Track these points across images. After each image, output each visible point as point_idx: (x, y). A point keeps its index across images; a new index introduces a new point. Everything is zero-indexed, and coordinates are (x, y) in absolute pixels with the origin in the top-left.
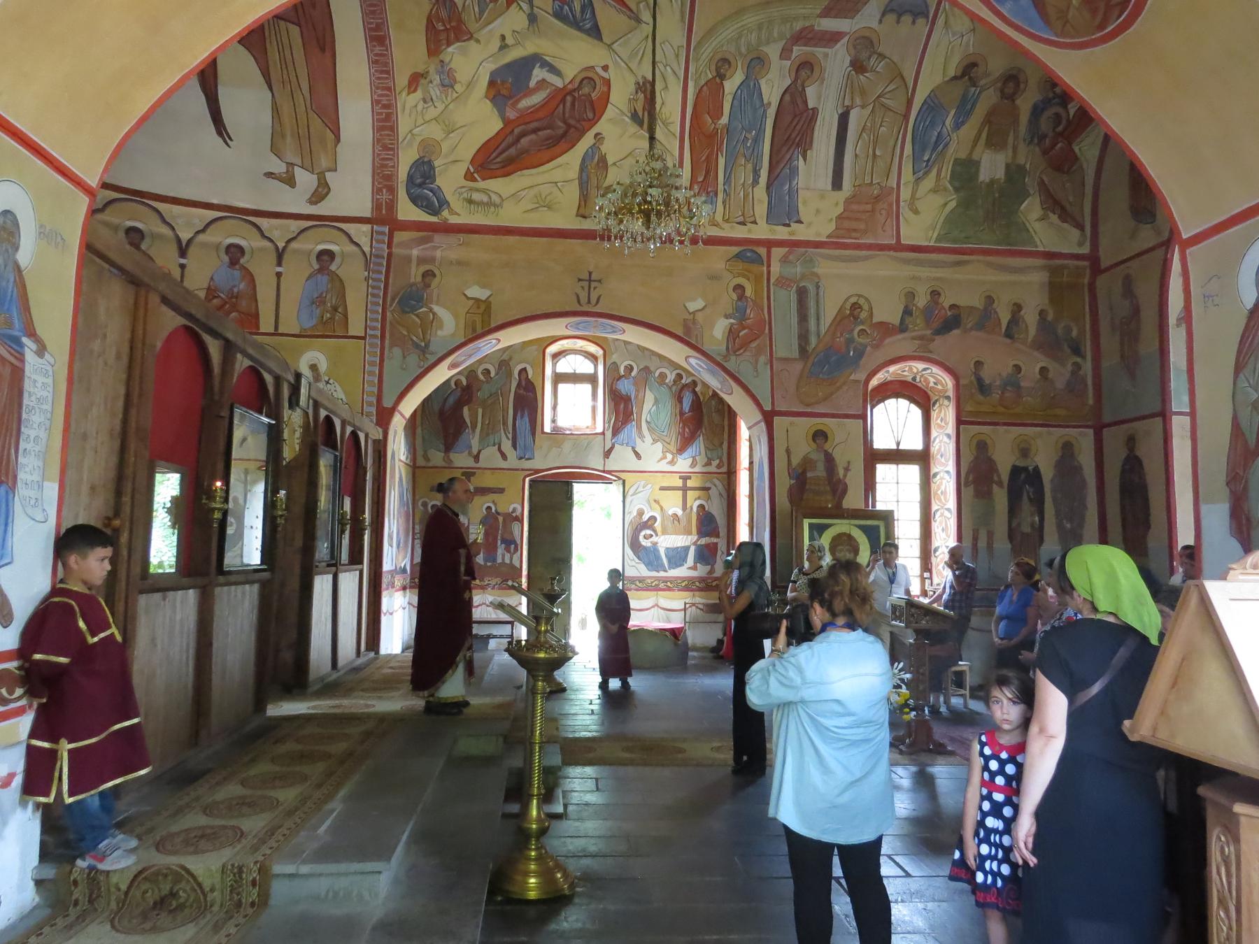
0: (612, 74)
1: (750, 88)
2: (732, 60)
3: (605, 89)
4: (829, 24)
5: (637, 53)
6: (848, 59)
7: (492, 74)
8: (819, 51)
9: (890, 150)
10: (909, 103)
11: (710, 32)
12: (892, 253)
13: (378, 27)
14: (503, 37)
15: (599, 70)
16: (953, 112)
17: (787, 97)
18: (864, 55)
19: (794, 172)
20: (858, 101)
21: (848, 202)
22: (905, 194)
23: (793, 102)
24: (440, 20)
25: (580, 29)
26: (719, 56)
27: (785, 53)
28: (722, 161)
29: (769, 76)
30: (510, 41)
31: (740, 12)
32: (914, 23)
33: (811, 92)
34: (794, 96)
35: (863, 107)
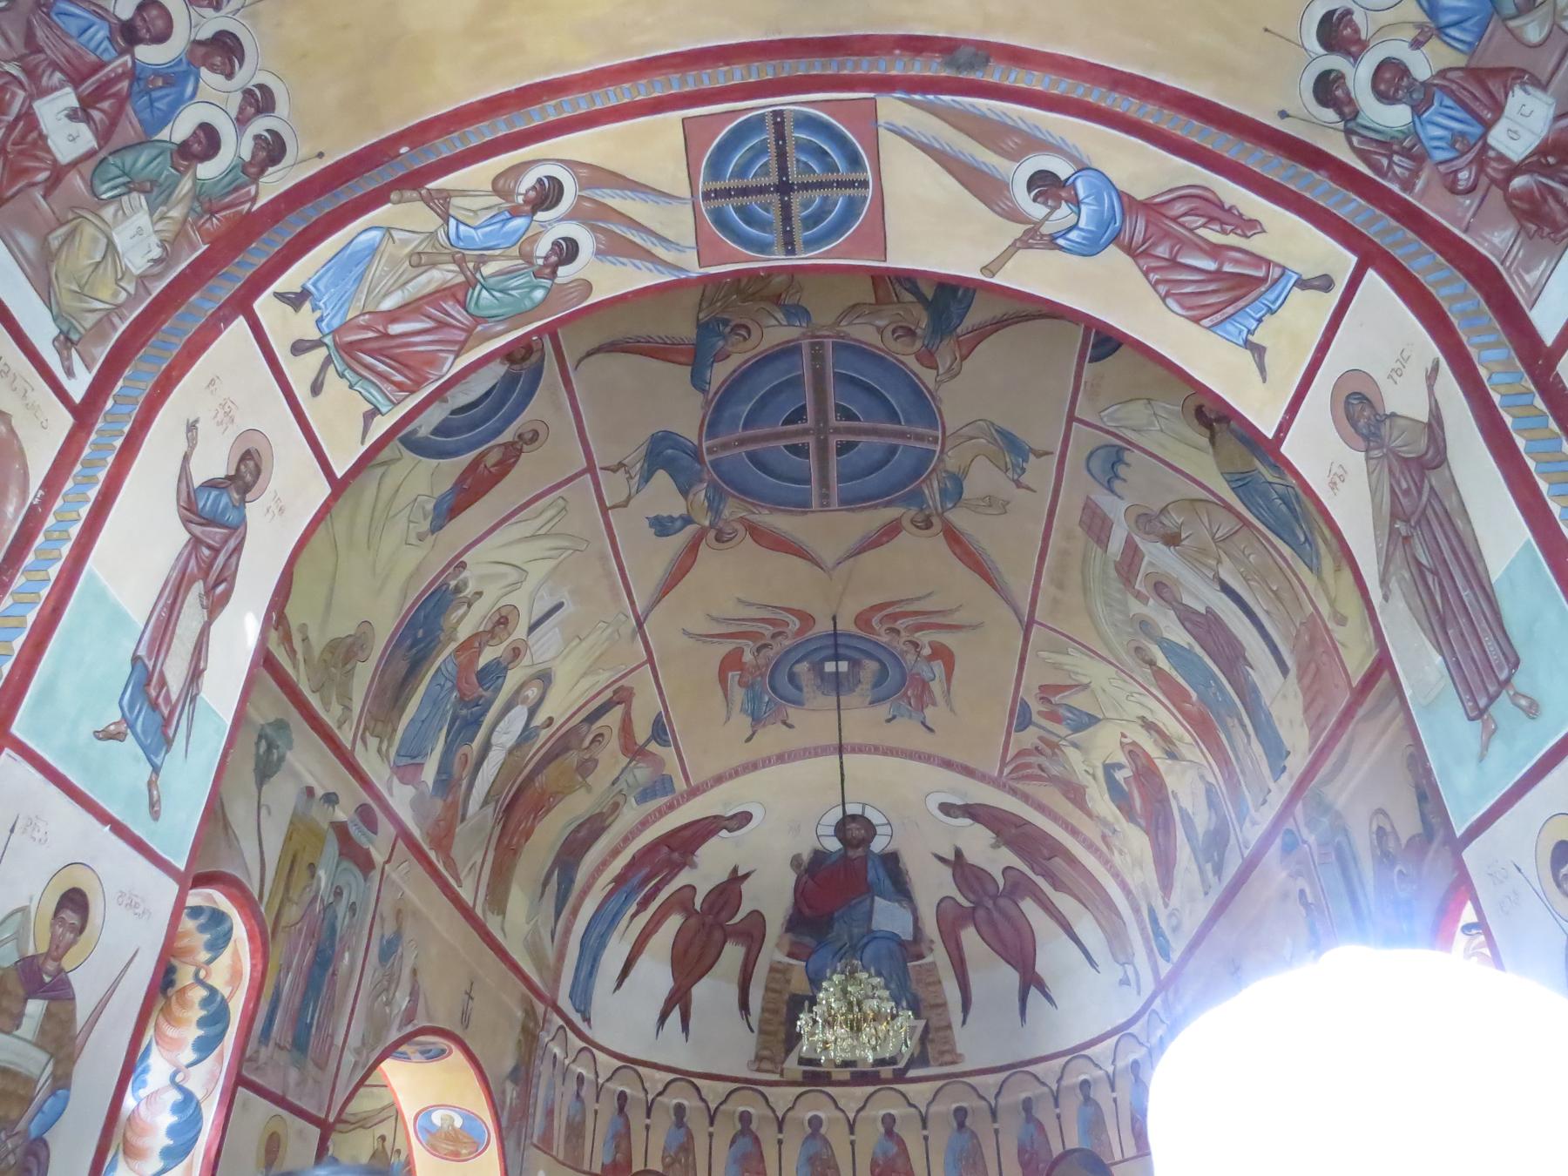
1: (1170, 649)
4: (1116, 545)
9: (1276, 570)
10: (1229, 508)
11: (1106, 644)
12: (1361, 712)
16: (1257, 463)
19: (1255, 689)
21: (1300, 679)
22: (1325, 609)
23: (1195, 624)
28: (1223, 737)
29: (1162, 626)
32: (1127, 465)
33: (1187, 600)
34: (1187, 617)
35: (1219, 562)
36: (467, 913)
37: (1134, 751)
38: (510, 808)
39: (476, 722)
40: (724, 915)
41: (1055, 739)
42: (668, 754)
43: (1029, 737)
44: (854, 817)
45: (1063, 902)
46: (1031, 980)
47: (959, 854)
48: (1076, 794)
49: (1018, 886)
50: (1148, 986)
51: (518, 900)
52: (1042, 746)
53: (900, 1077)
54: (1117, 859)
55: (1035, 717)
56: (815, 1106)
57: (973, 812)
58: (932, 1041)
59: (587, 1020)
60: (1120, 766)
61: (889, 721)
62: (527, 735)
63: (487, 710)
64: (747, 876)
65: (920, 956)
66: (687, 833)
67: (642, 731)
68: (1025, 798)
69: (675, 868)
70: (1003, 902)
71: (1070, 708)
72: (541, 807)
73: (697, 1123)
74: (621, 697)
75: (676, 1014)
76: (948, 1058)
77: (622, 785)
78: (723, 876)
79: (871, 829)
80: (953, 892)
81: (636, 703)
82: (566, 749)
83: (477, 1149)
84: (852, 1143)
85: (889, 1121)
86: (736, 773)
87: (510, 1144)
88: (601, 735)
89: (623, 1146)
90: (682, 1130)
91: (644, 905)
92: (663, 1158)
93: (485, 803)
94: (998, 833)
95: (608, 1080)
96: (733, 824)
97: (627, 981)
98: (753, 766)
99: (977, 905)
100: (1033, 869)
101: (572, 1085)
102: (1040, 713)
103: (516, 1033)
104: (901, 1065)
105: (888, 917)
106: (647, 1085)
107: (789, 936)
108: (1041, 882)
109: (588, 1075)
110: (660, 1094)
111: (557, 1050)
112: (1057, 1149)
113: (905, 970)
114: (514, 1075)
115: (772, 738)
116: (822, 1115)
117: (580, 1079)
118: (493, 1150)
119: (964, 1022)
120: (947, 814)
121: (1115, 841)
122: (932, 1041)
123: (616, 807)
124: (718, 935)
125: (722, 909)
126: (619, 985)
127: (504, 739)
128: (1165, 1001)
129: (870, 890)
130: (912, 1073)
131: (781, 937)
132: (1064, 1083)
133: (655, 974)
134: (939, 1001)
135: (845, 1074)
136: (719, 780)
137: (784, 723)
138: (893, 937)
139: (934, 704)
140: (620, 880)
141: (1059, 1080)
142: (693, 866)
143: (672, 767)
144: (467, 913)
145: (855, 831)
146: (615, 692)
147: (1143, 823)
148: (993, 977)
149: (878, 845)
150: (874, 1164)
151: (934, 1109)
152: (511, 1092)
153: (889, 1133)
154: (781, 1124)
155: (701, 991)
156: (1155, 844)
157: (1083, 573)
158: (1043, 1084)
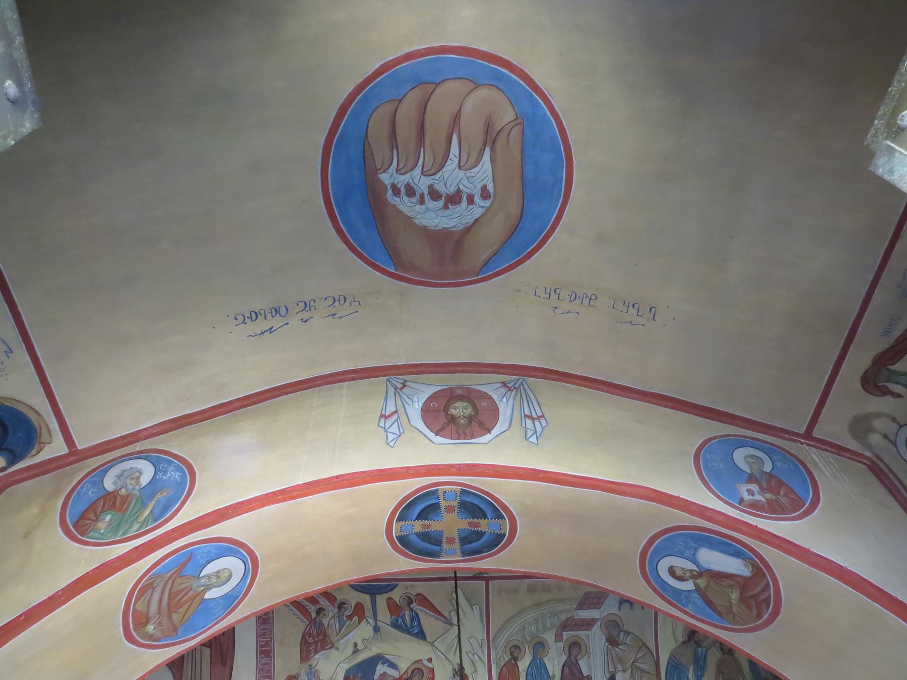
0: (435, 665)
1: (538, 666)
2: (521, 647)
3: (431, 676)
5: (452, 647)
6: (604, 640)
7: (348, 671)
8: (582, 634)
13: (267, 644)
14: (356, 645)
15: (426, 662)
16: (691, 668)
17: (566, 669)
18: (615, 634)
20: (620, 668)
23: (572, 673)
24: (310, 635)
25: (410, 633)
26: (510, 645)
27: (558, 638)
30: (360, 646)
31: (520, 612)
33: (582, 663)
35: (624, 671)
41: (368, 612)
55: (381, 600)
60: (393, 665)
71: (415, 617)
157: (549, 601)
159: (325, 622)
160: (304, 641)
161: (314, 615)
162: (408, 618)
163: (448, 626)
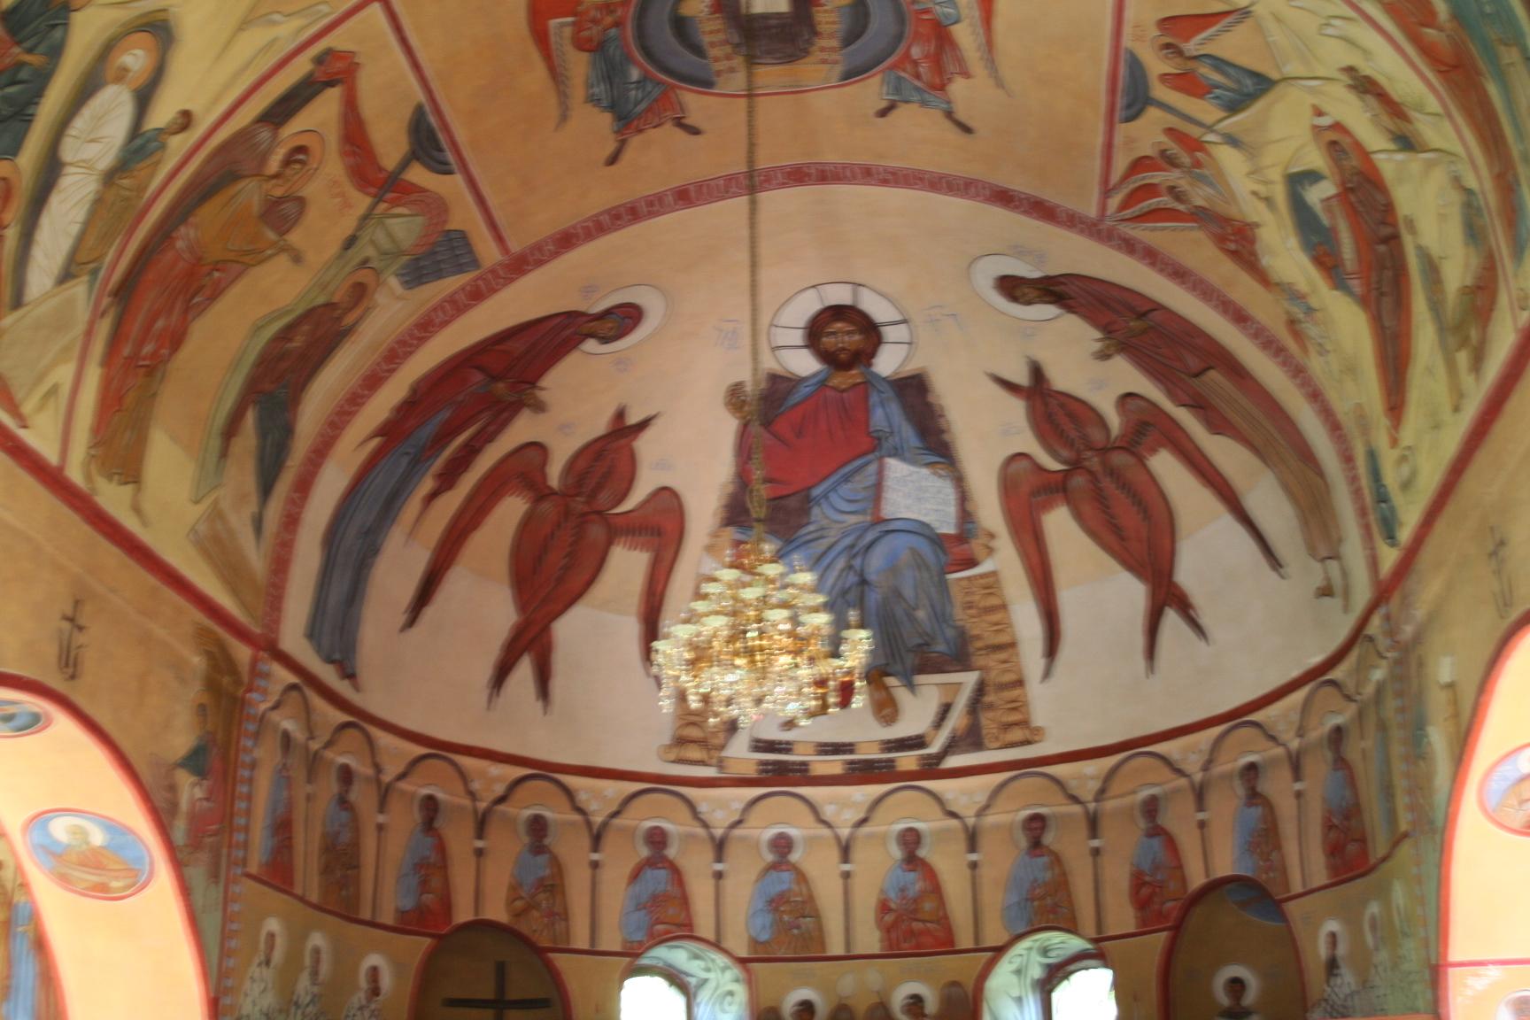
28: (1493, 90)
36: (52, 478)
37: (1337, 141)
38: (126, 292)
39: (22, 114)
40: (604, 497)
41: (1195, 131)
42: (450, 186)
43: (1147, 134)
44: (837, 312)
45: (1225, 453)
46: (1167, 596)
47: (1037, 372)
48: (1238, 241)
49: (1148, 428)
50: (1362, 593)
51: (170, 464)
52: (1174, 148)
53: (931, 769)
54: (1315, 364)
56: (781, 816)
57: (1055, 290)
58: (991, 707)
59: (350, 675)
60: (1312, 176)
61: (883, 113)
62: (140, 147)
63: (37, 94)
64: (643, 425)
65: (972, 563)
66: (517, 346)
67: (390, 143)
68: (1151, 256)
69: (504, 412)
70: (1119, 459)
71: (1219, 63)
72: (198, 285)
73: (572, 850)
74: (334, 72)
75: (524, 671)
76: (1017, 734)
77: (365, 250)
78: (599, 425)
79: (871, 332)
80: (1027, 442)
81: (369, 85)
82: (234, 177)
83: (138, 882)
84: (846, 876)
85: (911, 840)
86: (598, 227)
87: (197, 874)
88: (301, 149)
89: (436, 882)
90: (542, 859)
91: (447, 480)
92: (511, 901)
93: (66, 276)
94: (1107, 330)
95: (402, 776)
96: (606, 327)
97: (429, 613)
98: (630, 214)
99: (1076, 465)
100: (1172, 395)
101: (329, 786)
102: (1164, 78)
103: (194, 691)
104: (934, 749)
105: (913, 493)
106: (476, 786)
107: (731, 533)
108: (1185, 417)
109: (361, 767)
110: (502, 799)
111: (288, 725)
112: (1197, 880)
113: (943, 586)
114: (195, 761)
115: (659, 157)
116: (793, 832)
117: (346, 775)
118: (163, 882)
119: (1047, 674)
120: (1014, 298)
121: (1312, 330)
122: (991, 707)
123: (360, 292)
124: (596, 532)
125: (599, 487)
126: (412, 621)
127: (91, 151)
128: (1388, 618)
129: (875, 446)
130: (953, 762)
131: (715, 535)
132: (1219, 769)
133: (482, 601)
134: (1003, 639)
135: (833, 765)
136: (566, 241)
137: (679, 123)
138: (922, 530)
139: (966, 74)
140: (391, 432)
141: (1206, 767)
142: (540, 407)
143: (465, 216)
144: (52, 478)
145: (843, 337)
146: (319, 60)
147: (1356, 285)
148: (1103, 594)
149: (887, 363)
150: (884, 907)
151: (990, 819)
152: (190, 790)
153: (912, 860)
154: (720, 848)
155: (570, 629)
156: (1377, 321)
158: (1180, 772)
159: (1200, 202)
160: (1235, 255)
161: (1181, 207)
162: (1216, 77)
163: (1249, 22)
